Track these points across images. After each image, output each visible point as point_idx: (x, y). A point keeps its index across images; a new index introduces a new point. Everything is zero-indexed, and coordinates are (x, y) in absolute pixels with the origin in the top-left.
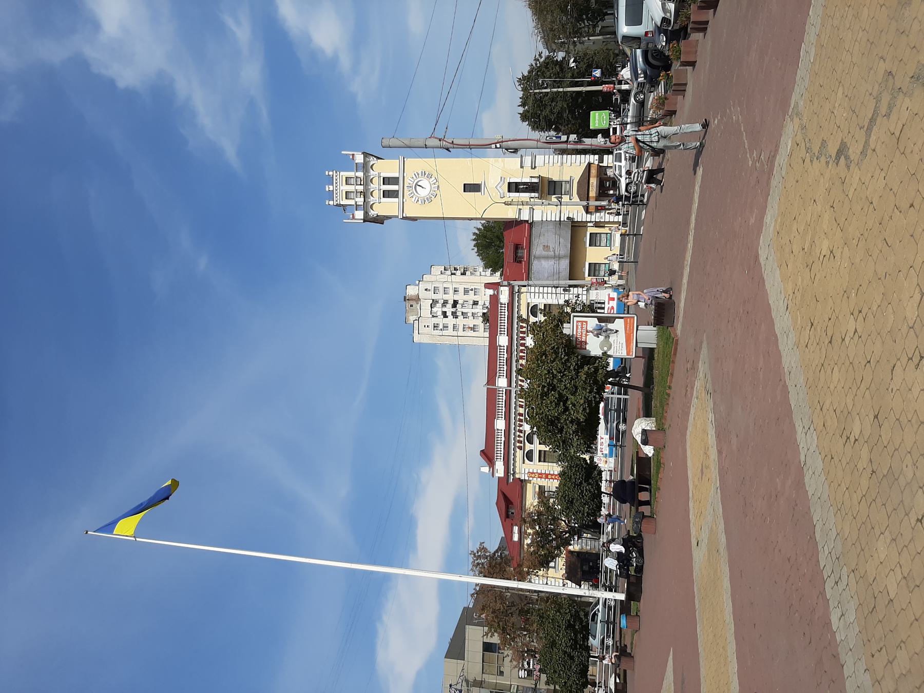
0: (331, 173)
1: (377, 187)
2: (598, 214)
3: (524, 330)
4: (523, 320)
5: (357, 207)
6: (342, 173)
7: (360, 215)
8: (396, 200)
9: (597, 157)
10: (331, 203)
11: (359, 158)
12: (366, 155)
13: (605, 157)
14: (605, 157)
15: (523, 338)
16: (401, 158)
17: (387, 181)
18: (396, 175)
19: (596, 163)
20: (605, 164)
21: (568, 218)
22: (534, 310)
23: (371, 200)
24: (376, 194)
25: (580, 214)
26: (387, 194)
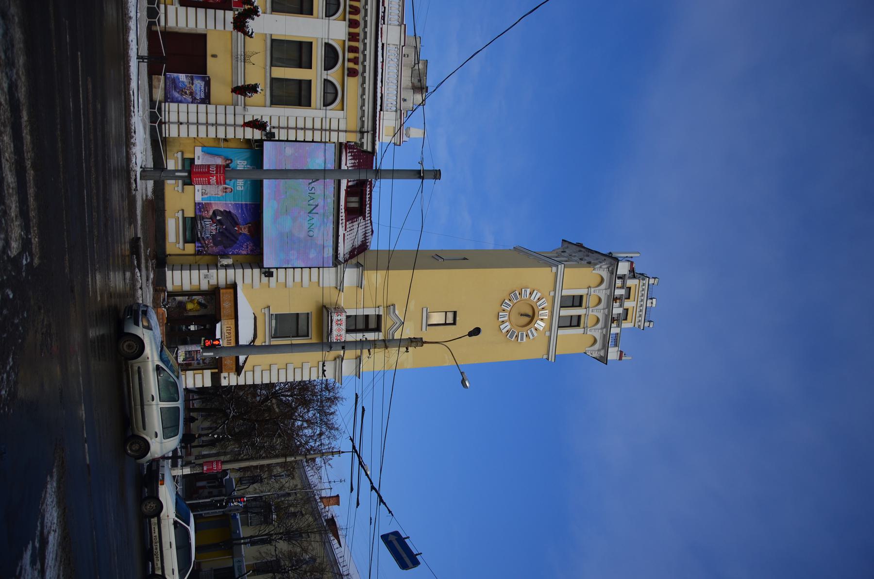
0: (647, 324)
1: (591, 313)
2: (213, 282)
3: (352, 55)
4: (353, 73)
5: (622, 277)
6: (631, 325)
7: (623, 268)
8: (566, 293)
9: (224, 383)
10: (652, 281)
11: (613, 354)
12: (604, 360)
13: (208, 383)
14: (208, 383)
15: (353, 37)
16: (552, 358)
17: (575, 322)
18: (562, 332)
19: (223, 375)
20: (208, 373)
21: (269, 274)
22: (331, 95)
23: (602, 292)
24: (593, 301)
25: (248, 280)
26: (577, 301)
